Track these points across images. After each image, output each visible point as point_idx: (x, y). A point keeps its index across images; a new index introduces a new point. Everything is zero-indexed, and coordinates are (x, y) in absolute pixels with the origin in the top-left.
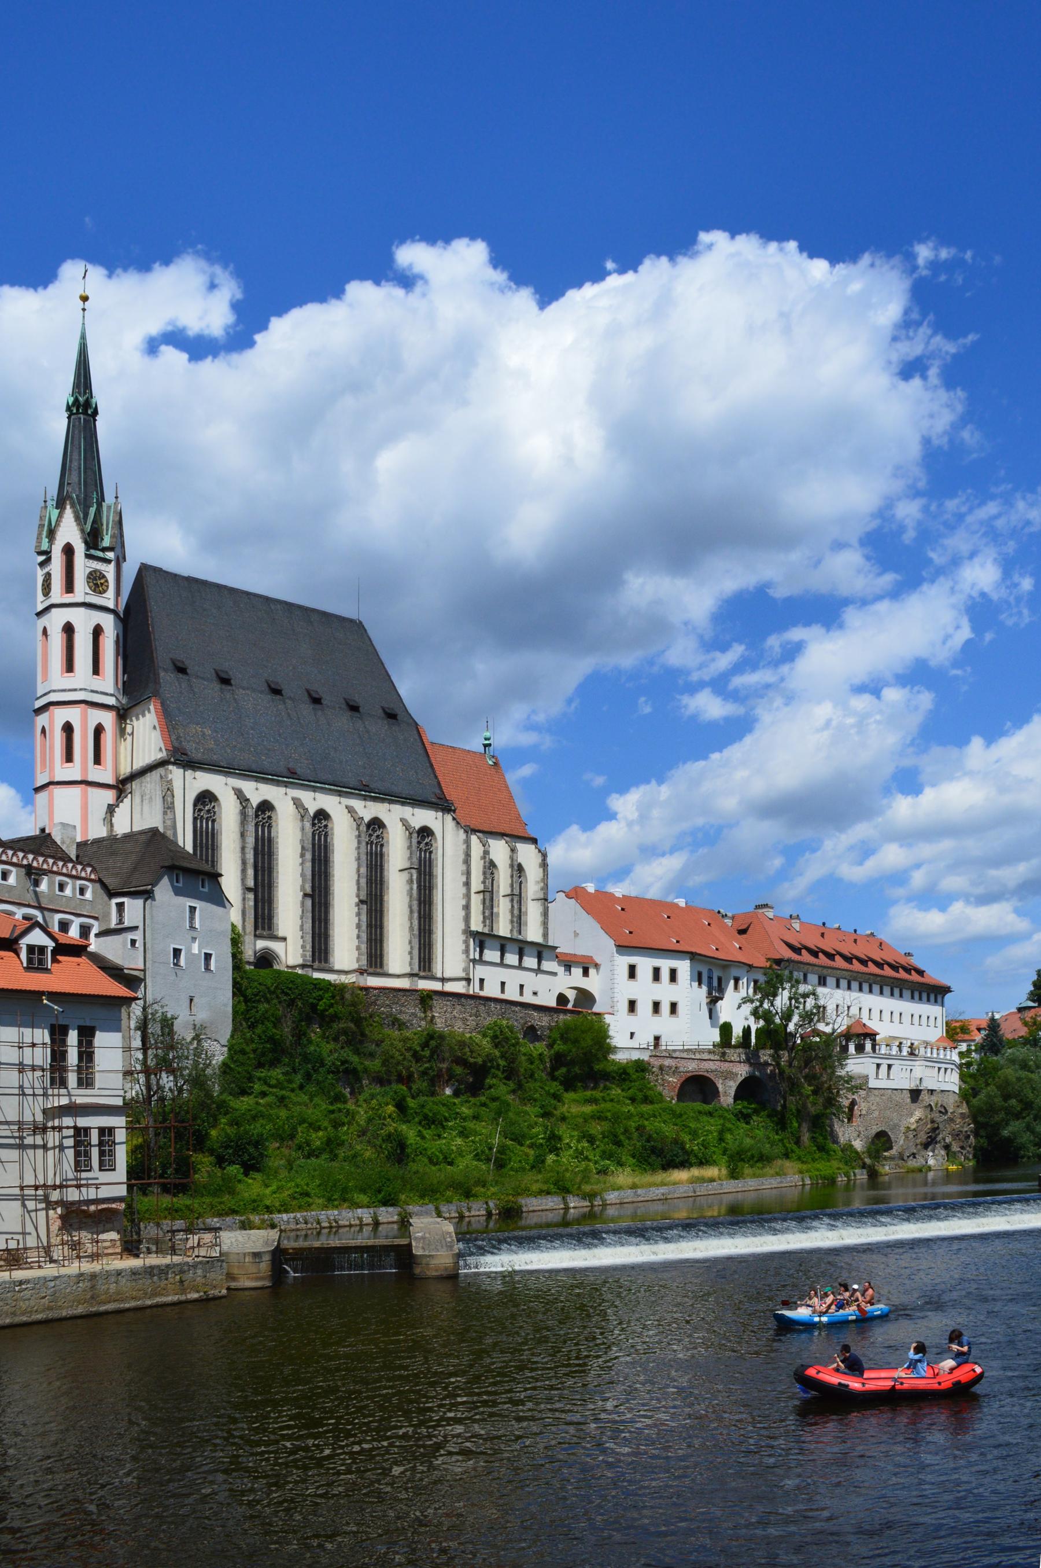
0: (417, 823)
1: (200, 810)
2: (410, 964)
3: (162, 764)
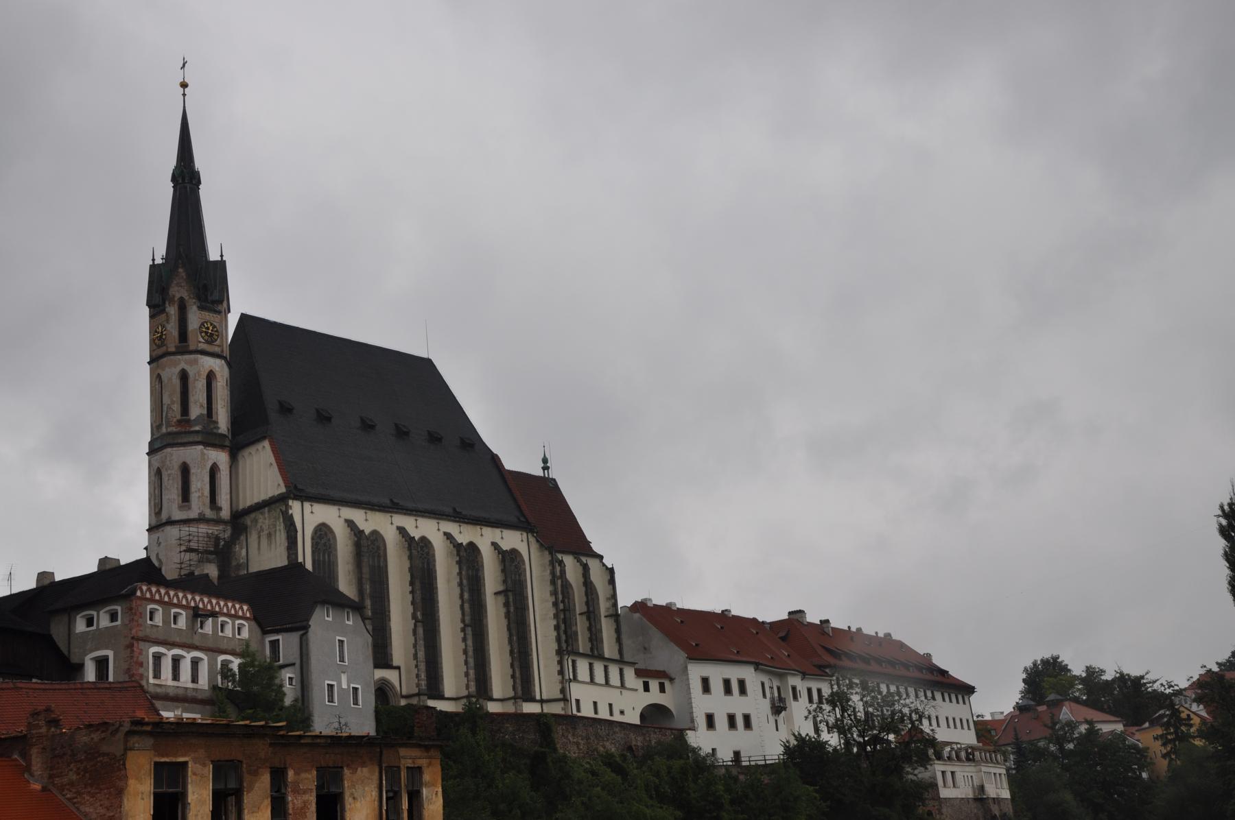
0: (505, 546)
2: (514, 688)
3: (281, 500)
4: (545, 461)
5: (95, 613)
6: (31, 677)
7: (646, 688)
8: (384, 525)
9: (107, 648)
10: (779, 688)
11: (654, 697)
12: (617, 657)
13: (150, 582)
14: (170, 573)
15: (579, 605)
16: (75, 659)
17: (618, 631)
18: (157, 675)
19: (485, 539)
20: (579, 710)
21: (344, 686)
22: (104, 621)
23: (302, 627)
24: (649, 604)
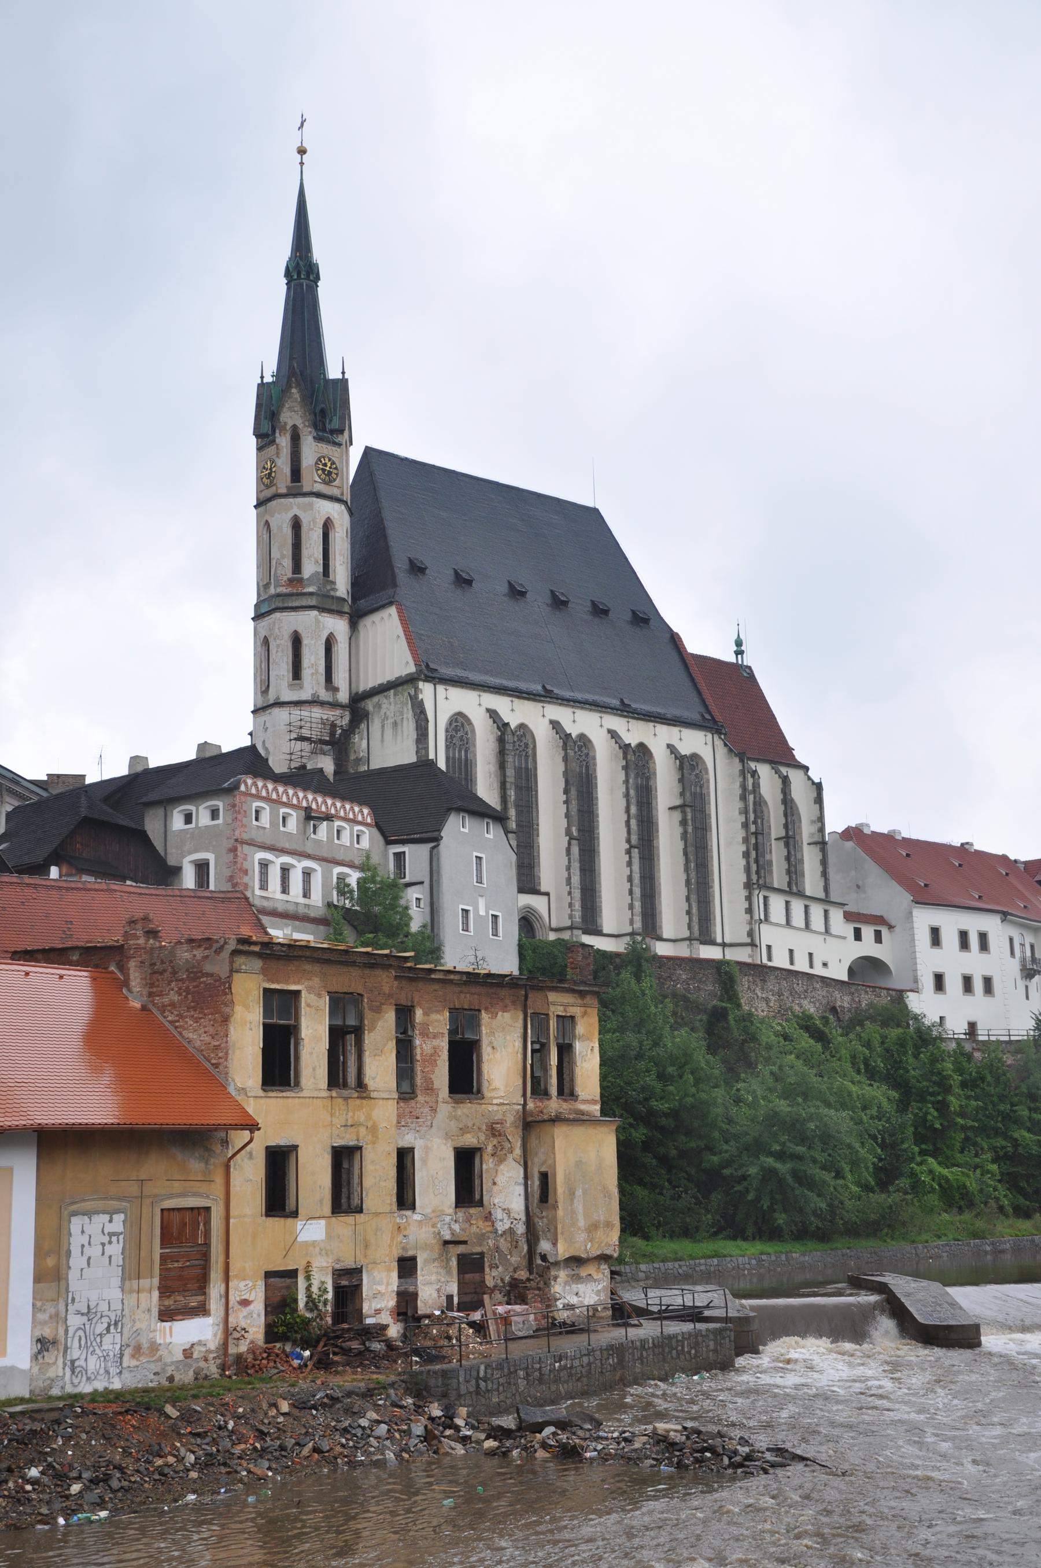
0: (685, 750)
1: (452, 737)
2: (690, 927)
3: (410, 680)
4: (739, 643)
5: (193, 808)
6: (124, 879)
7: (858, 935)
8: (535, 718)
9: (207, 851)
10: (1032, 947)
11: (868, 947)
12: (821, 895)
13: (256, 775)
14: (279, 764)
15: (776, 826)
16: (172, 861)
17: (824, 862)
18: (264, 886)
19: (658, 739)
20: (770, 959)
21: (482, 913)
22: (203, 818)
23: (435, 840)
24: (866, 831)
